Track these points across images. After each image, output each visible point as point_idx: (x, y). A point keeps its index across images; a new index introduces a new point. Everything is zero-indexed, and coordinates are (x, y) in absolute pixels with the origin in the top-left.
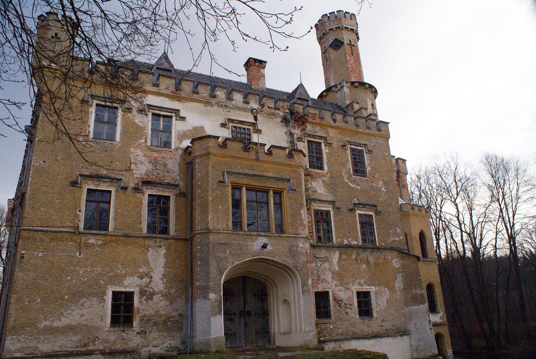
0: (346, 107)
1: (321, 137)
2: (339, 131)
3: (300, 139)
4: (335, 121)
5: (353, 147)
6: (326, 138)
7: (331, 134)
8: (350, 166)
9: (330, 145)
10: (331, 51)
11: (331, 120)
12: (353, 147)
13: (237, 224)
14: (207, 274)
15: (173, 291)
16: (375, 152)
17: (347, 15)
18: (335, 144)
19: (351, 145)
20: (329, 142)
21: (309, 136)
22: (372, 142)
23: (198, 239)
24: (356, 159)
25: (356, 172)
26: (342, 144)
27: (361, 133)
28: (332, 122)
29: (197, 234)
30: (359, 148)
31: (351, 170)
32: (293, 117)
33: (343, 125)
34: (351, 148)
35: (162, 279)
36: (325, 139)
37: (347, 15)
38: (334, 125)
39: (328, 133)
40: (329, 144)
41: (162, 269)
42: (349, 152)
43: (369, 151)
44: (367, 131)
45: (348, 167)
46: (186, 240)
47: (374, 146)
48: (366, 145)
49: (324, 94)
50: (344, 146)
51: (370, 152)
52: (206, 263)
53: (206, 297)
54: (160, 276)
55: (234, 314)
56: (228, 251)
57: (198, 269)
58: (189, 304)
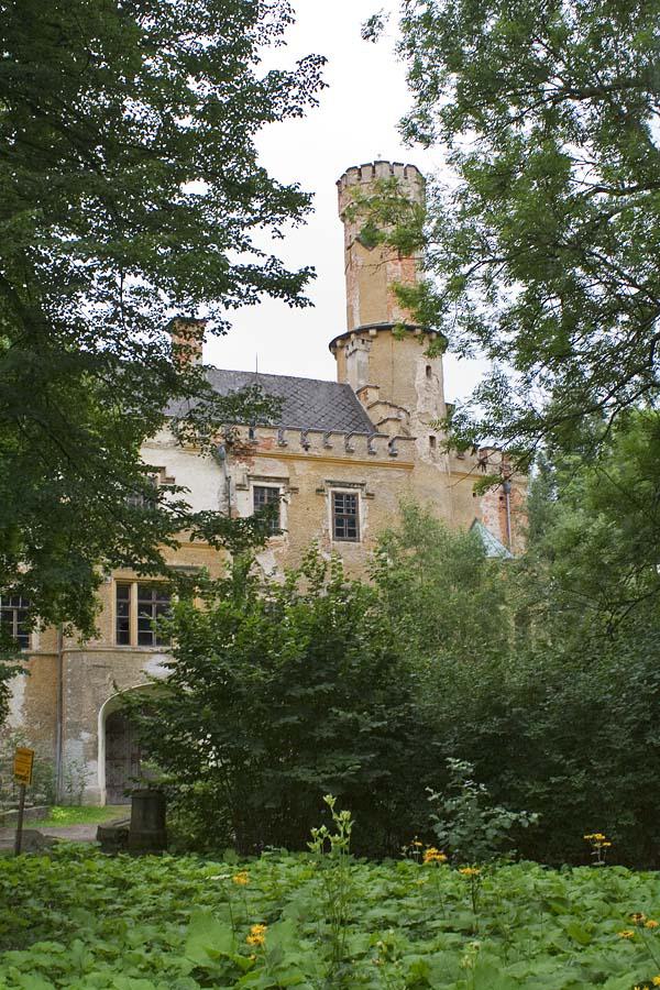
0: (358, 392)
1: (278, 479)
2: (313, 463)
3: (241, 487)
4: (307, 447)
5: (339, 490)
6: (288, 479)
7: (297, 472)
8: (330, 525)
9: (294, 490)
10: (358, 248)
11: (300, 446)
12: (339, 490)
13: (123, 638)
14: (79, 709)
15: (37, 727)
16: (381, 495)
17: (396, 168)
18: (304, 488)
19: (335, 486)
20: (292, 485)
21: (258, 478)
22: (373, 479)
23: (68, 659)
24: (341, 511)
25: (339, 533)
26: (319, 486)
27: (356, 463)
28: (302, 450)
29: (68, 652)
30: (350, 491)
31: (331, 532)
32: (231, 449)
33: (323, 453)
34: (334, 493)
35: (22, 712)
36: (286, 480)
37: (396, 168)
38: (306, 454)
39: (292, 470)
40: (292, 489)
41: (22, 697)
42: (329, 501)
43: (368, 494)
44: (369, 458)
45: (324, 527)
46: (55, 655)
47: (380, 485)
48: (363, 485)
49: (338, 343)
50: (319, 491)
51: (370, 496)
52: (78, 693)
53: (77, 737)
54: (19, 707)
55: (124, 758)
56: (109, 676)
57: (67, 701)
58: (58, 745)
